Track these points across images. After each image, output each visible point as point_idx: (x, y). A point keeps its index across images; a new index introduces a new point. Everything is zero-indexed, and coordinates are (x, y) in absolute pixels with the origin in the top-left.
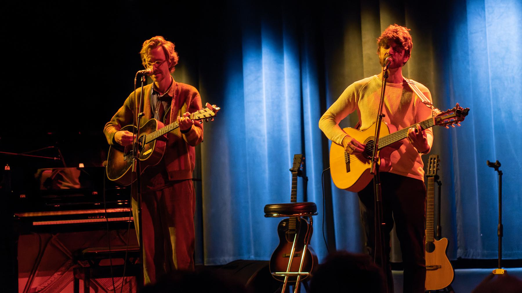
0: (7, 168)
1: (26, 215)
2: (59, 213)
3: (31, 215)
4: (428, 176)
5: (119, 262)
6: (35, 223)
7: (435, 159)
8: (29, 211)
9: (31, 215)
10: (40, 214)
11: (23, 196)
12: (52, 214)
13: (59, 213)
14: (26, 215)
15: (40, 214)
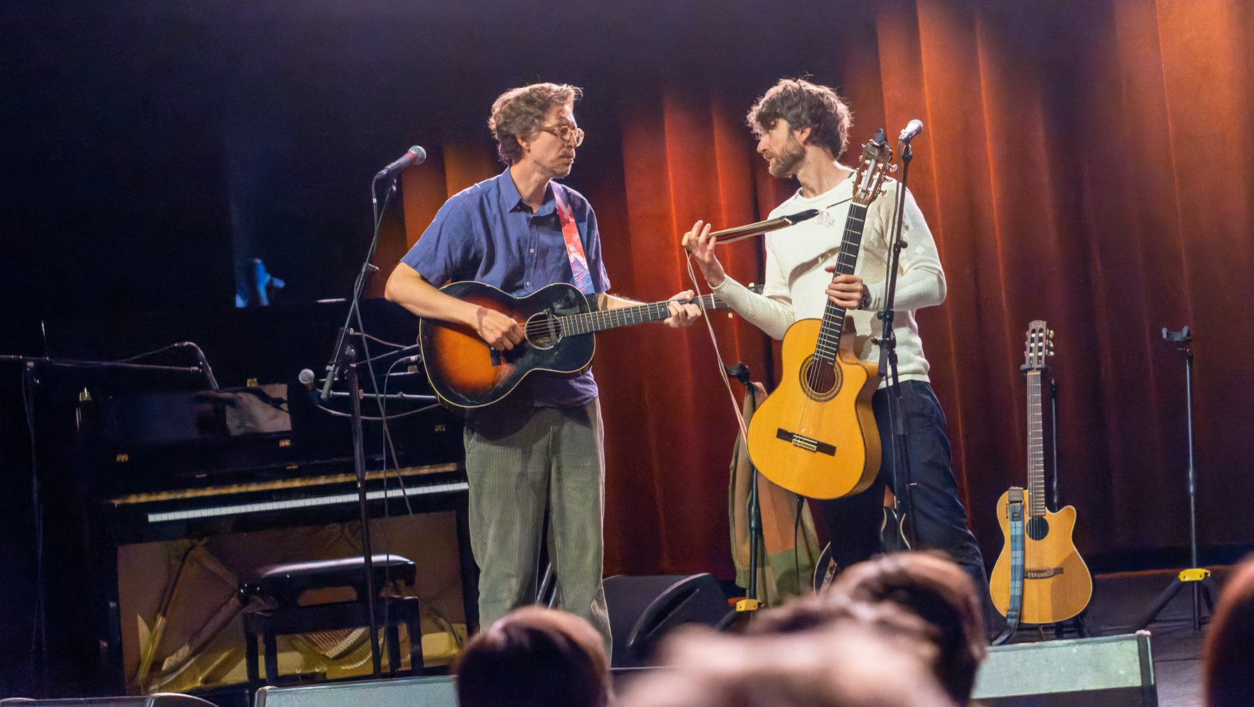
0: (86, 394)
1: (133, 500)
2: (209, 492)
3: (144, 498)
4: (1026, 371)
5: (348, 593)
6: (153, 518)
7: (1041, 331)
8: (138, 492)
9: (144, 498)
10: (164, 497)
11: (123, 458)
12: (189, 494)
13: (209, 492)
14: (133, 500)
15: (164, 497)
